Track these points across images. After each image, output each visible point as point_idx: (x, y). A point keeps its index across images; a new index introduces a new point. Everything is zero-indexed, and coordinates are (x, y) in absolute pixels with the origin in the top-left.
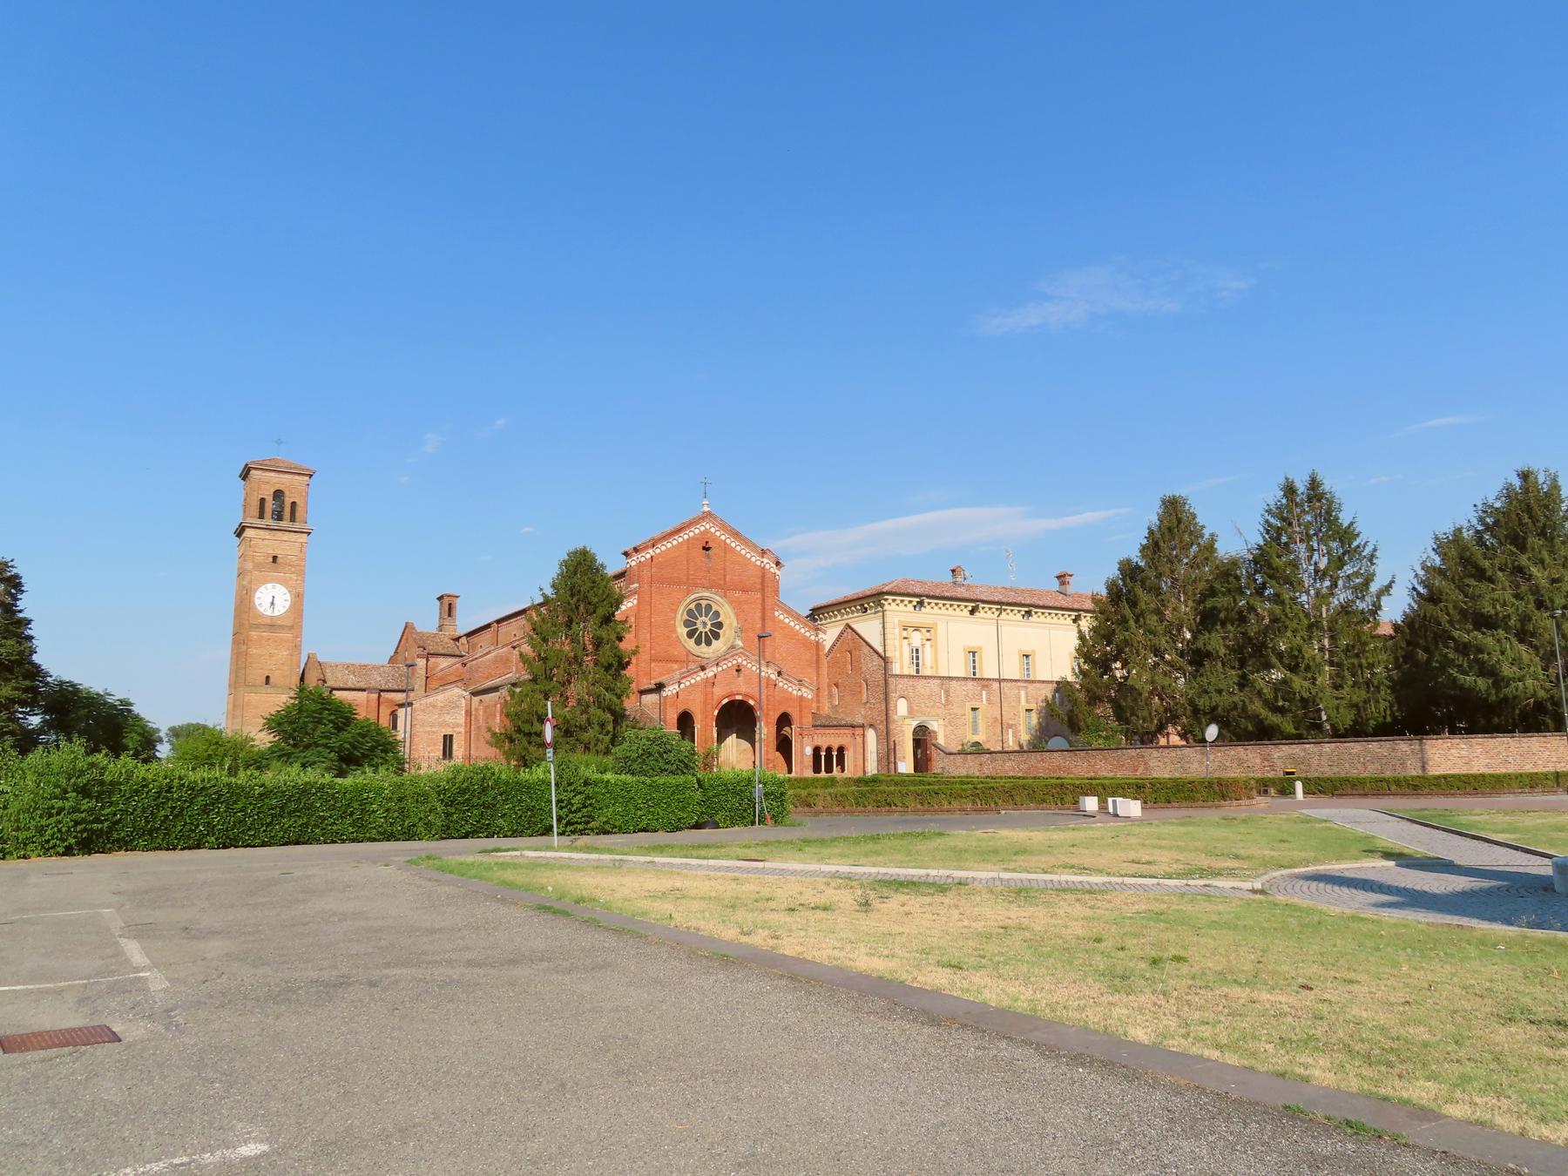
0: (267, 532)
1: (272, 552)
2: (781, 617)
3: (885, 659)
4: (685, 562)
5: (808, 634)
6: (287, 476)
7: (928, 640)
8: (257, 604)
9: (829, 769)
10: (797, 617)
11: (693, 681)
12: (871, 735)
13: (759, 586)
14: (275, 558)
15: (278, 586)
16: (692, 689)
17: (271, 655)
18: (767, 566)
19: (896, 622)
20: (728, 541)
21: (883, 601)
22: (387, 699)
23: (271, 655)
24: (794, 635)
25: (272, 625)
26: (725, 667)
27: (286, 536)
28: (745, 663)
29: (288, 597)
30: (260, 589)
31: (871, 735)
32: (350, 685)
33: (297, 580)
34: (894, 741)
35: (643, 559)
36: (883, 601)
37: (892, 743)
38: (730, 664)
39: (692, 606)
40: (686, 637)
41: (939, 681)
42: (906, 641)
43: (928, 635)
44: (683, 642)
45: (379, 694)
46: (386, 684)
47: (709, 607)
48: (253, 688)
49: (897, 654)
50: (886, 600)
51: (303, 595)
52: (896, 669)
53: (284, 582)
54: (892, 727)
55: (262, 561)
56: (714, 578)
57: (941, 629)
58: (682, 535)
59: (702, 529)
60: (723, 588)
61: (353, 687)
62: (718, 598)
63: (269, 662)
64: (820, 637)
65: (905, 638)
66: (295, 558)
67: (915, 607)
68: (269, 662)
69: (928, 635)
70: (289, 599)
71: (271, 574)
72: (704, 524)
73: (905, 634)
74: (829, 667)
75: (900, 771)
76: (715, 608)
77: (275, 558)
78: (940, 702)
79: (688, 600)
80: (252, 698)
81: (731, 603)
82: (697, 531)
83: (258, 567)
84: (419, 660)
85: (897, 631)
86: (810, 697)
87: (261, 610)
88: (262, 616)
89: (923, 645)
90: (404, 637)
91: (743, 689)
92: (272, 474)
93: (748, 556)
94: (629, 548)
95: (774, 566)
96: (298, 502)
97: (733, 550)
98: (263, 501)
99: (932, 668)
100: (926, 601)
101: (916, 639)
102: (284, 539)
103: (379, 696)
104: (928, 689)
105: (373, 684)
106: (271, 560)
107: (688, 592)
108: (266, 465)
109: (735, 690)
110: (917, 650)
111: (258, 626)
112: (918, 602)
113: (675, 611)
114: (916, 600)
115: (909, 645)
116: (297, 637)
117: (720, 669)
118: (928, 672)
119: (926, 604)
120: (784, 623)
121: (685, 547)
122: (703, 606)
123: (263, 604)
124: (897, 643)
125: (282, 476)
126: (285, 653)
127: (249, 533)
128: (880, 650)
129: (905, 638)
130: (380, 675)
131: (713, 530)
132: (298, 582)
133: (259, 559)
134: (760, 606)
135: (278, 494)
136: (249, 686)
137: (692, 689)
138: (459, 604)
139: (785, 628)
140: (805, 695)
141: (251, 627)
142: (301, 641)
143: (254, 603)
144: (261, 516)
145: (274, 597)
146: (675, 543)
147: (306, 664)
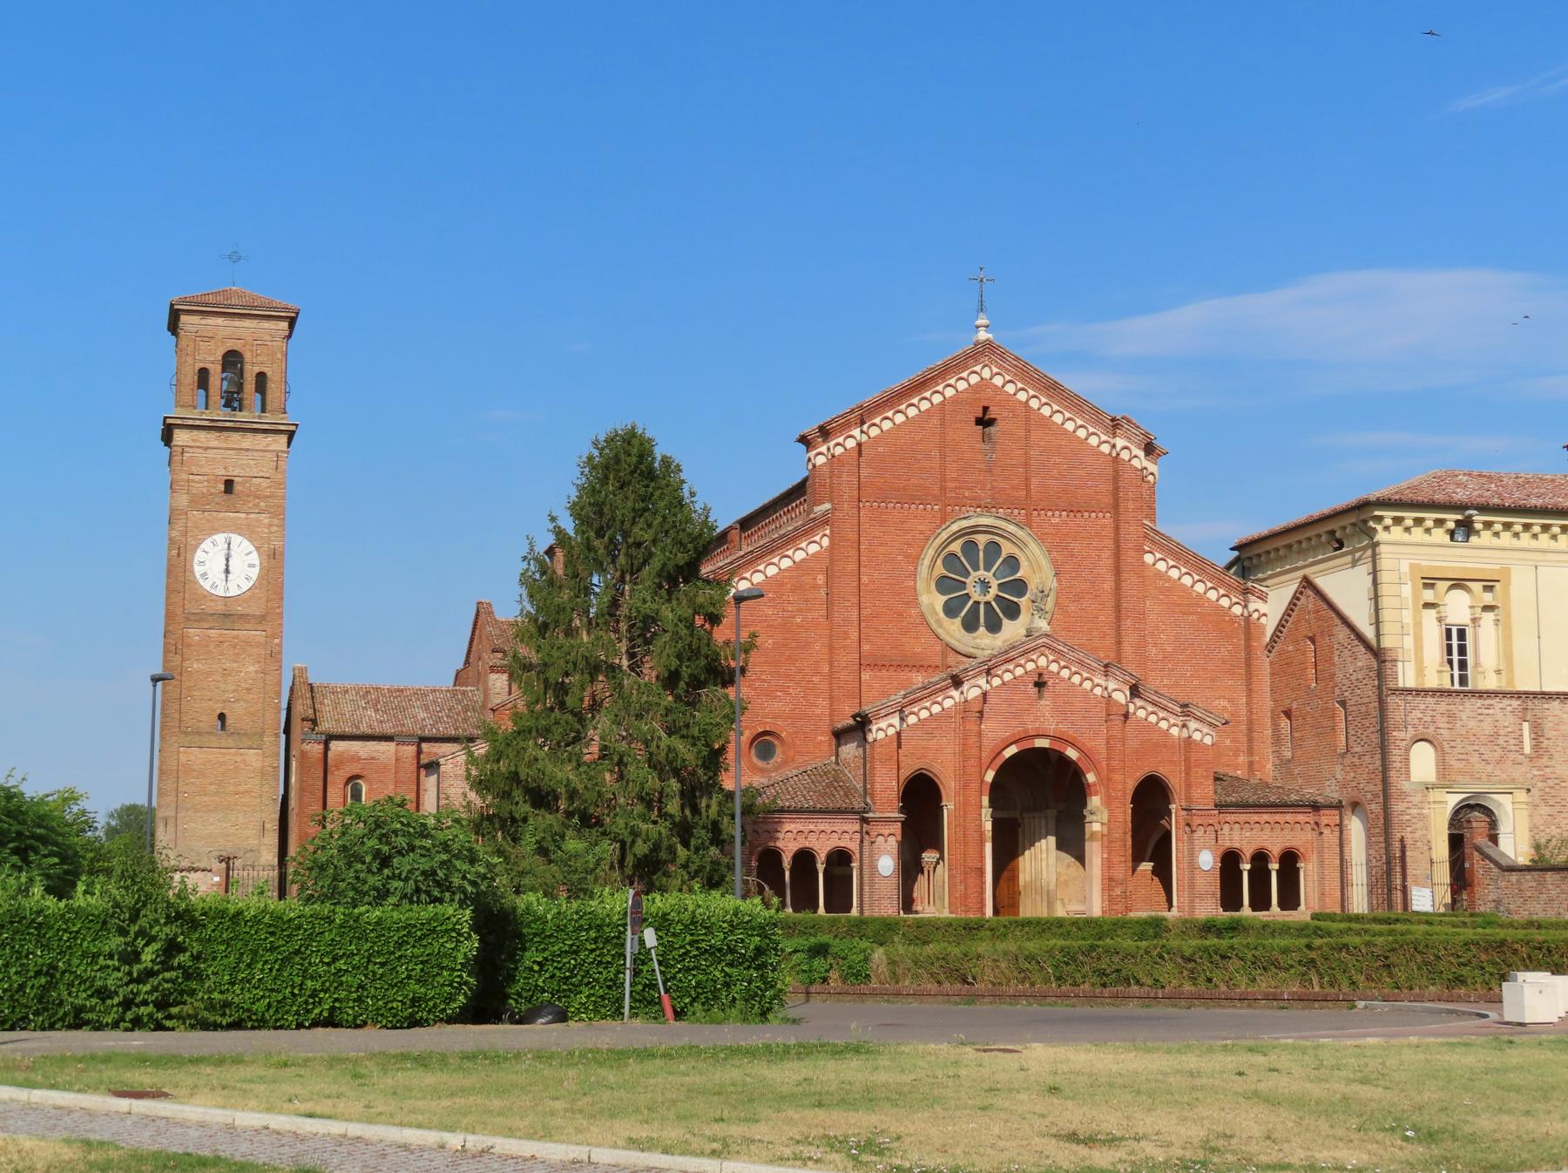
0: (214, 434)
1: (222, 472)
2: (1161, 566)
3: (1377, 653)
4: (936, 453)
5: (1225, 602)
6: (247, 323)
7: (1487, 608)
8: (198, 575)
9: (1261, 902)
10: (1198, 564)
11: (936, 709)
12: (1355, 828)
13: (1107, 500)
14: (229, 485)
16: (934, 725)
17: (226, 673)
18: (1125, 455)
19: (1405, 567)
20: (1034, 404)
21: (1371, 524)
23: (226, 673)
24: (1192, 603)
25: (228, 615)
26: (1008, 677)
27: (248, 441)
28: (1054, 667)
29: (255, 558)
30: (203, 546)
31: (1355, 828)
32: (364, 729)
33: (271, 525)
34: (1402, 840)
35: (839, 450)
36: (1371, 524)
37: (1397, 845)
38: (1019, 671)
39: (956, 547)
40: (942, 615)
41: (1515, 703)
42: (1431, 614)
43: (1488, 598)
44: (934, 626)
45: (419, 747)
46: (433, 726)
47: (994, 548)
49: (1409, 642)
50: (1380, 519)
51: (282, 554)
52: (1406, 676)
53: (248, 531)
54: (1397, 807)
55: (205, 491)
56: (1002, 485)
57: (1520, 584)
58: (927, 394)
59: (974, 379)
60: (1027, 507)
61: (368, 731)
62: (1011, 528)
64: (1252, 607)
65: (1427, 605)
66: (265, 483)
67: (1452, 533)
69: (1488, 598)
70: (257, 562)
71: (221, 515)
72: (977, 368)
73: (1429, 596)
74: (1273, 674)
75: (1416, 907)
76: (1007, 548)
77: (229, 485)
78: (1520, 751)
79: (944, 535)
80: (195, 756)
81: (1041, 539)
82: (962, 385)
83: (197, 502)
84: (493, 676)
85: (1407, 590)
86: (1208, 741)
87: (206, 585)
88: (208, 596)
89: (1474, 620)
91: (1051, 726)
92: (220, 321)
93: (1082, 433)
94: (810, 427)
95: (1141, 454)
96: (269, 374)
97: (1046, 423)
99: (1498, 672)
100: (1479, 519)
101: (1458, 607)
102: (245, 445)
103: (327, 748)
104: (1488, 720)
105: (409, 725)
106: (222, 487)
107: (944, 519)
108: (207, 305)
109: (1031, 727)
110: (1462, 634)
111: (200, 618)
112: (1458, 522)
113: (915, 560)
114: (1451, 518)
115: (1440, 620)
116: (274, 636)
117: (996, 682)
118: (1490, 682)
119: (1478, 526)
120: (1169, 579)
121: (936, 421)
122: (981, 547)
124: (1407, 617)
125: (237, 323)
126: (252, 668)
127: (180, 437)
128: (1369, 633)
129: (1427, 605)
130: (426, 708)
131: (998, 381)
132: (274, 529)
133: (200, 487)
134: (1109, 543)
135: (232, 360)
136: (186, 733)
137: (934, 725)
139: (1169, 589)
140: (1197, 736)
141: (188, 619)
142: (280, 645)
143: (192, 572)
146: (912, 412)
147: (292, 690)
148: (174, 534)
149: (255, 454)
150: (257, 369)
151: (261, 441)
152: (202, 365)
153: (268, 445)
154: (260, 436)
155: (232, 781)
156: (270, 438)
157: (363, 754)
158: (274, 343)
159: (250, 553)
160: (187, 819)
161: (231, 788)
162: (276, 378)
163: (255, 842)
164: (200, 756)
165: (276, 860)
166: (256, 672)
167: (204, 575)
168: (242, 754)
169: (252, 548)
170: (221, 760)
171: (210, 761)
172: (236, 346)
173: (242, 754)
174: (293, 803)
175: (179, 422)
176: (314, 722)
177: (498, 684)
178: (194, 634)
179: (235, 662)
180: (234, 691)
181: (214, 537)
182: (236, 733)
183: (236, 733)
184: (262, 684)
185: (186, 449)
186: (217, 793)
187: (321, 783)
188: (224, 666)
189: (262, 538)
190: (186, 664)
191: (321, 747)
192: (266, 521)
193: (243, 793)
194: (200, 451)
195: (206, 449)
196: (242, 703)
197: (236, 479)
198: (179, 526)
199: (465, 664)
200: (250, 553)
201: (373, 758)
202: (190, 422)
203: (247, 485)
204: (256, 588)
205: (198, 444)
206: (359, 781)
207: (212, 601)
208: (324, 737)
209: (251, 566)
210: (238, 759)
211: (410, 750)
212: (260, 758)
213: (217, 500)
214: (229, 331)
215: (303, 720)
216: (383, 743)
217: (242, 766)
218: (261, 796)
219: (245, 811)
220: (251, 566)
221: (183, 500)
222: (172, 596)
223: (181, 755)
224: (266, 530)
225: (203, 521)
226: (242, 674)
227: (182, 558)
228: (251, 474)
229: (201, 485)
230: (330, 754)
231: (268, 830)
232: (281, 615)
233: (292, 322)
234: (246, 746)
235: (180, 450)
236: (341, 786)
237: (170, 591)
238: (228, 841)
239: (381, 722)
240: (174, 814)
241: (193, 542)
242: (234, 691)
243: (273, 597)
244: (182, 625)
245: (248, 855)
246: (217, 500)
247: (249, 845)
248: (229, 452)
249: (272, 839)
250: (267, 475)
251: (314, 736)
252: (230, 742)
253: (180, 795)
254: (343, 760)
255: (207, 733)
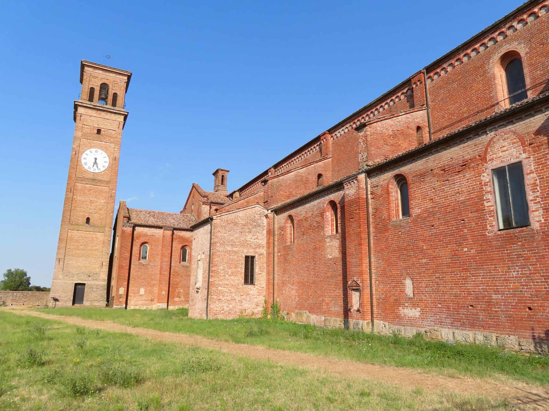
6: (111, 75)
14: (99, 131)
15: (100, 151)
17: (91, 202)
22: (179, 236)
23: (91, 202)
25: (94, 180)
29: (107, 159)
30: (86, 152)
32: (150, 223)
33: (114, 148)
45: (173, 231)
46: (178, 225)
48: (76, 227)
51: (119, 159)
53: (105, 149)
55: (89, 132)
61: (152, 224)
63: (90, 207)
66: (113, 132)
68: (90, 207)
70: (108, 161)
71: (95, 142)
77: (99, 131)
80: (75, 234)
83: (85, 136)
84: (204, 206)
87: (86, 167)
88: (86, 171)
90: (191, 196)
92: (101, 72)
96: (118, 94)
98: (92, 90)
102: (106, 117)
105: (168, 223)
106: (96, 132)
108: (96, 64)
111: (83, 179)
116: (112, 189)
123: (88, 163)
127: (80, 110)
130: (174, 219)
132: (116, 149)
133: (87, 130)
135: (104, 87)
136: (72, 225)
138: (228, 176)
142: (115, 193)
143: (81, 161)
144: (91, 99)
145: (96, 159)
147: (118, 211)
148: (74, 146)
149: (110, 121)
150: (114, 92)
151: (113, 117)
152: (92, 86)
153: (116, 119)
154: (113, 115)
155: (90, 245)
156: (117, 116)
157: (149, 234)
158: (121, 83)
159: (106, 157)
160: (69, 259)
161: (90, 248)
162: (121, 96)
163: (98, 270)
164: (77, 234)
165: (107, 278)
166: (104, 203)
167: (86, 163)
168: (95, 234)
169: (107, 156)
170: (86, 236)
171: (81, 236)
172: (107, 82)
173: (95, 234)
174: (116, 254)
175: (80, 104)
176: (129, 219)
177: (206, 210)
178: (79, 185)
179: (96, 198)
180: (94, 209)
181: (91, 149)
182: (94, 226)
183: (94, 226)
184: (106, 208)
185: (82, 115)
186: (83, 250)
187: (130, 244)
188: (91, 199)
189: (111, 152)
190: (75, 197)
191: (132, 229)
192: (113, 146)
193: (95, 250)
194: (88, 117)
195: (91, 116)
196: (97, 214)
197: (102, 129)
198: (77, 143)
199: (184, 209)
200: (106, 157)
201: (153, 236)
202: (85, 105)
203: (107, 132)
204: (107, 171)
205: (88, 114)
206: (146, 245)
207: (88, 173)
208: (133, 225)
209: (106, 162)
210: (94, 236)
211: (169, 233)
212: (103, 236)
213: (93, 136)
214: (103, 76)
215: (124, 217)
216: (158, 229)
217: (95, 239)
218: (102, 252)
219: (95, 257)
220: (106, 162)
221: (79, 134)
222: (71, 170)
223: (69, 233)
224: (112, 150)
225: (87, 143)
226: (98, 203)
227: (77, 155)
228: (108, 128)
229: (87, 129)
230: (135, 233)
231: (104, 265)
232: (116, 182)
233: (129, 77)
234: (97, 231)
235: (80, 115)
236: (139, 247)
237: (71, 168)
238: (87, 269)
239: (157, 222)
240: (63, 257)
241: (82, 150)
242: (94, 209)
243: (113, 174)
244: (74, 182)
245: (95, 275)
246: (93, 136)
247: (95, 271)
248: (100, 119)
249: (106, 269)
250: (115, 130)
251: (128, 224)
252: (91, 229)
253: (67, 249)
254: (140, 236)
255: (81, 225)
